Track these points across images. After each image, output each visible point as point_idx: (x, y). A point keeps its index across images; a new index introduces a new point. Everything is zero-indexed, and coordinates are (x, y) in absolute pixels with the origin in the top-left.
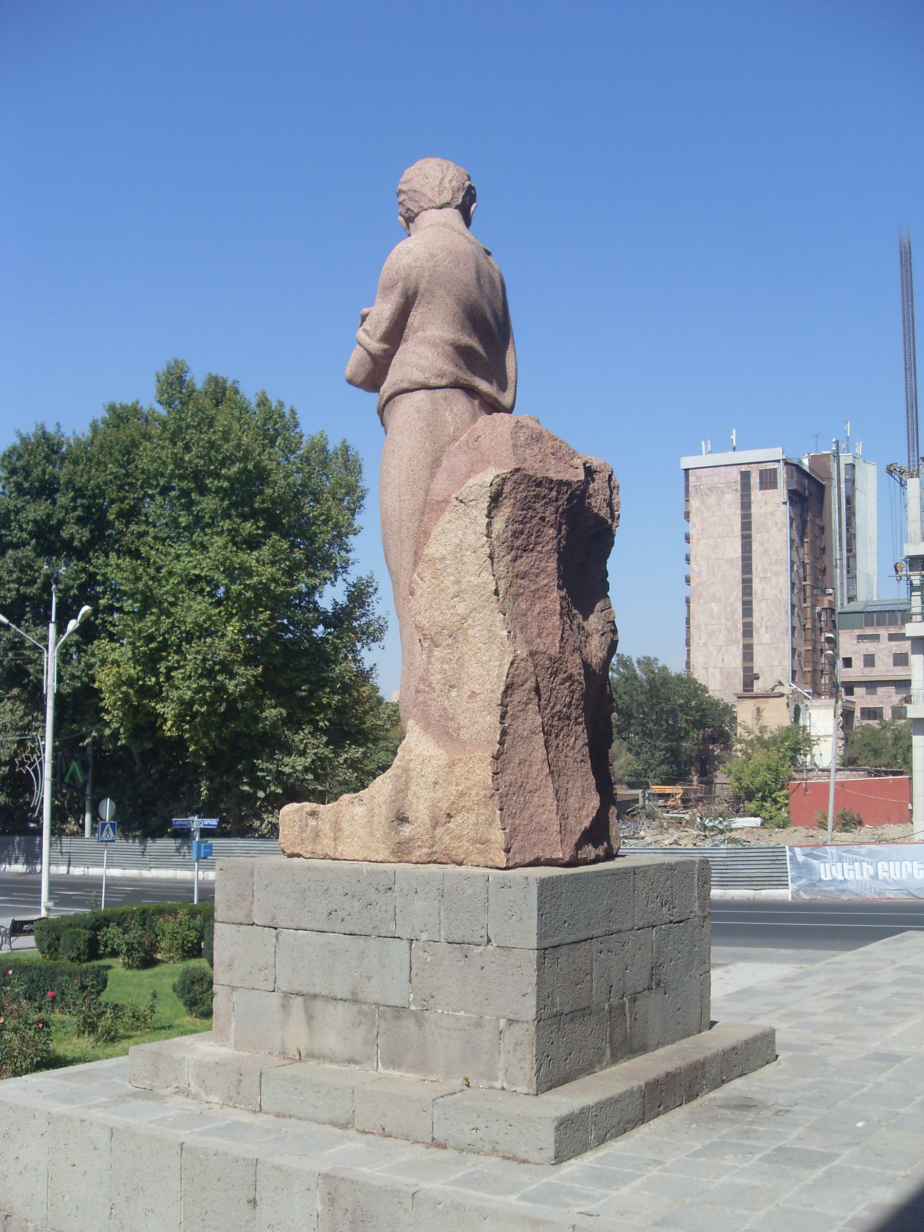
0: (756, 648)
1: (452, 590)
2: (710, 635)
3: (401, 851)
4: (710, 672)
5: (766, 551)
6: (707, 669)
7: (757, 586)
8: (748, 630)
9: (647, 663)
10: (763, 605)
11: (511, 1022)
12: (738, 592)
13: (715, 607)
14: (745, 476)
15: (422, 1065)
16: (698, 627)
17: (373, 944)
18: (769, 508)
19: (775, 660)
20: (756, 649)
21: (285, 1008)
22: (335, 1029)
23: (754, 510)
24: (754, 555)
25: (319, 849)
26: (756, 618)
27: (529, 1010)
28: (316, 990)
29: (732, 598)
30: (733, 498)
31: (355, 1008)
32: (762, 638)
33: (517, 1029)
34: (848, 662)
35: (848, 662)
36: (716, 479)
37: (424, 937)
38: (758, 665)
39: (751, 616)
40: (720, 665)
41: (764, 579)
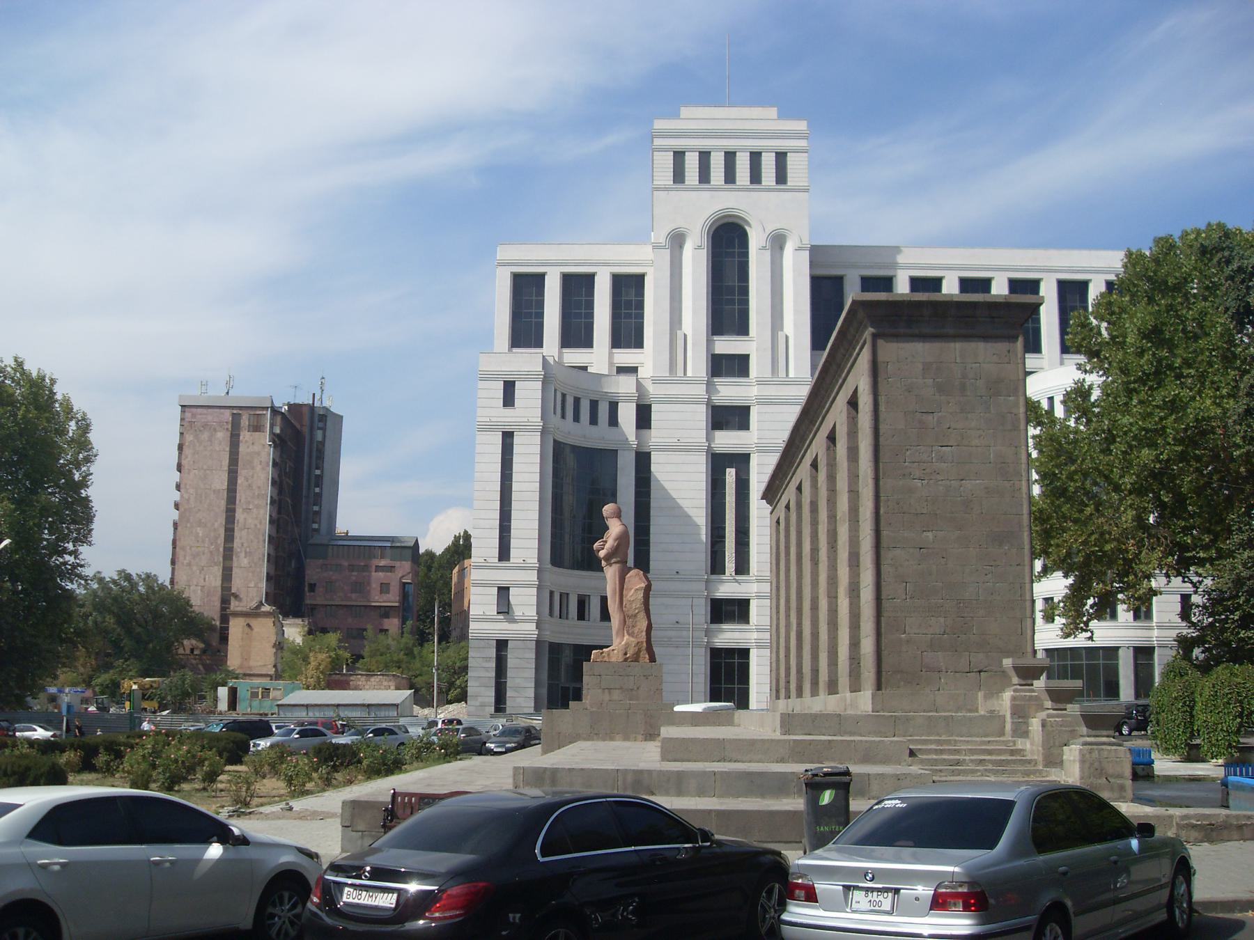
0: (235, 570)
2: (195, 556)
3: (626, 660)
5: (250, 486)
7: (240, 515)
8: (228, 554)
9: (149, 578)
10: (244, 533)
12: (221, 520)
13: (200, 531)
14: (236, 419)
16: (183, 548)
18: (256, 448)
19: (252, 582)
20: (236, 572)
22: (616, 695)
23: (242, 448)
24: (239, 488)
26: (237, 543)
29: (216, 525)
30: (222, 436)
32: (241, 562)
34: (312, 587)
35: (312, 587)
36: (210, 418)
38: (237, 584)
39: (232, 541)
40: (202, 582)
41: (247, 510)
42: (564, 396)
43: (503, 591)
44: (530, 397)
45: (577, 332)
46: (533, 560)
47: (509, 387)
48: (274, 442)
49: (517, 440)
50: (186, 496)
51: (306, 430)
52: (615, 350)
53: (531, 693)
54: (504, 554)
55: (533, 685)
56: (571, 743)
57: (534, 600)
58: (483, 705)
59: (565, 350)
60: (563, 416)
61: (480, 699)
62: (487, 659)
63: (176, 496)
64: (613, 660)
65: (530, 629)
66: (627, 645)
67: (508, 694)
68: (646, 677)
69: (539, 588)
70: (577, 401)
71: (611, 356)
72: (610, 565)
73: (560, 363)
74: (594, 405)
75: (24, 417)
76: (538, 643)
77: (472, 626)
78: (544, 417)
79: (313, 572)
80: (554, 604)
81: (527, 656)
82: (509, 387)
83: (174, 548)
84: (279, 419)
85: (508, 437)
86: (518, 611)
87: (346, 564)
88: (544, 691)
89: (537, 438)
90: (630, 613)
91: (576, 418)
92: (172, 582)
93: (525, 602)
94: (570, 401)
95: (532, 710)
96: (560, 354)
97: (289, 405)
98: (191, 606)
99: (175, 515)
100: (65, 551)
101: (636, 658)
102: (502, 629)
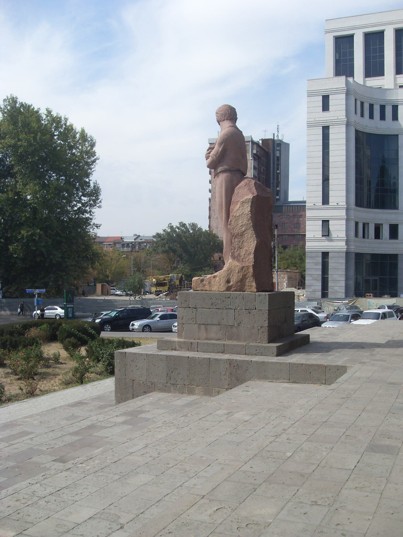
1: (240, 225)
3: (228, 289)
4: (219, 229)
6: (217, 228)
9: (194, 226)
11: (261, 327)
15: (238, 339)
16: (214, 211)
17: (225, 311)
21: (199, 328)
25: (205, 289)
27: (266, 324)
28: (208, 323)
31: (220, 326)
33: (263, 329)
37: (239, 308)
42: (362, 104)
43: (325, 223)
44: (338, 104)
45: (374, 68)
46: (343, 203)
47: (326, 99)
48: (254, 157)
49: (331, 131)
50: (214, 186)
51: (271, 151)
52: (398, 76)
53: (343, 284)
54: (326, 200)
55: (344, 279)
56: (145, 393)
57: (344, 227)
58: (314, 291)
59: (367, 79)
60: (362, 115)
61: (313, 288)
62: (316, 264)
63: (210, 186)
64: (215, 288)
65: (341, 245)
66: (230, 271)
67: (330, 284)
68: (249, 310)
69: (348, 220)
70: (371, 106)
71: (395, 79)
72: (216, 175)
73: (364, 86)
74: (383, 108)
75: (40, 139)
76: (348, 253)
77: (308, 244)
78: (347, 116)
79: (276, 219)
80: (359, 230)
81: (340, 261)
82: (326, 99)
83: (210, 210)
84: (255, 146)
85: (326, 130)
86: (334, 234)
87: (291, 215)
88: (352, 283)
89: (343, 129)
90: (236, 231)
91: (371, 117)
92: (209, 227)
93: (339, 229)
94: (366, 107)
95: (343, 296)
96: (364, 81)
97: (263, 140)
98: (218, 238)
99: (209, 195)
100: (86, 211)
101: (241, 286)
102: (325, 245)
